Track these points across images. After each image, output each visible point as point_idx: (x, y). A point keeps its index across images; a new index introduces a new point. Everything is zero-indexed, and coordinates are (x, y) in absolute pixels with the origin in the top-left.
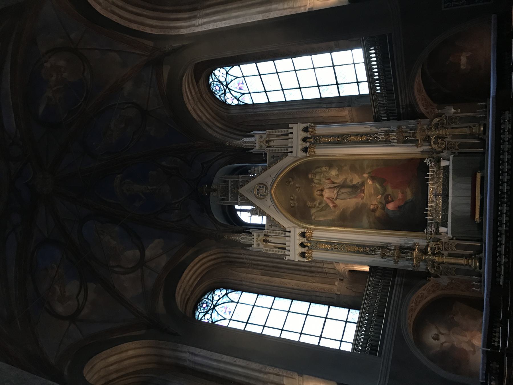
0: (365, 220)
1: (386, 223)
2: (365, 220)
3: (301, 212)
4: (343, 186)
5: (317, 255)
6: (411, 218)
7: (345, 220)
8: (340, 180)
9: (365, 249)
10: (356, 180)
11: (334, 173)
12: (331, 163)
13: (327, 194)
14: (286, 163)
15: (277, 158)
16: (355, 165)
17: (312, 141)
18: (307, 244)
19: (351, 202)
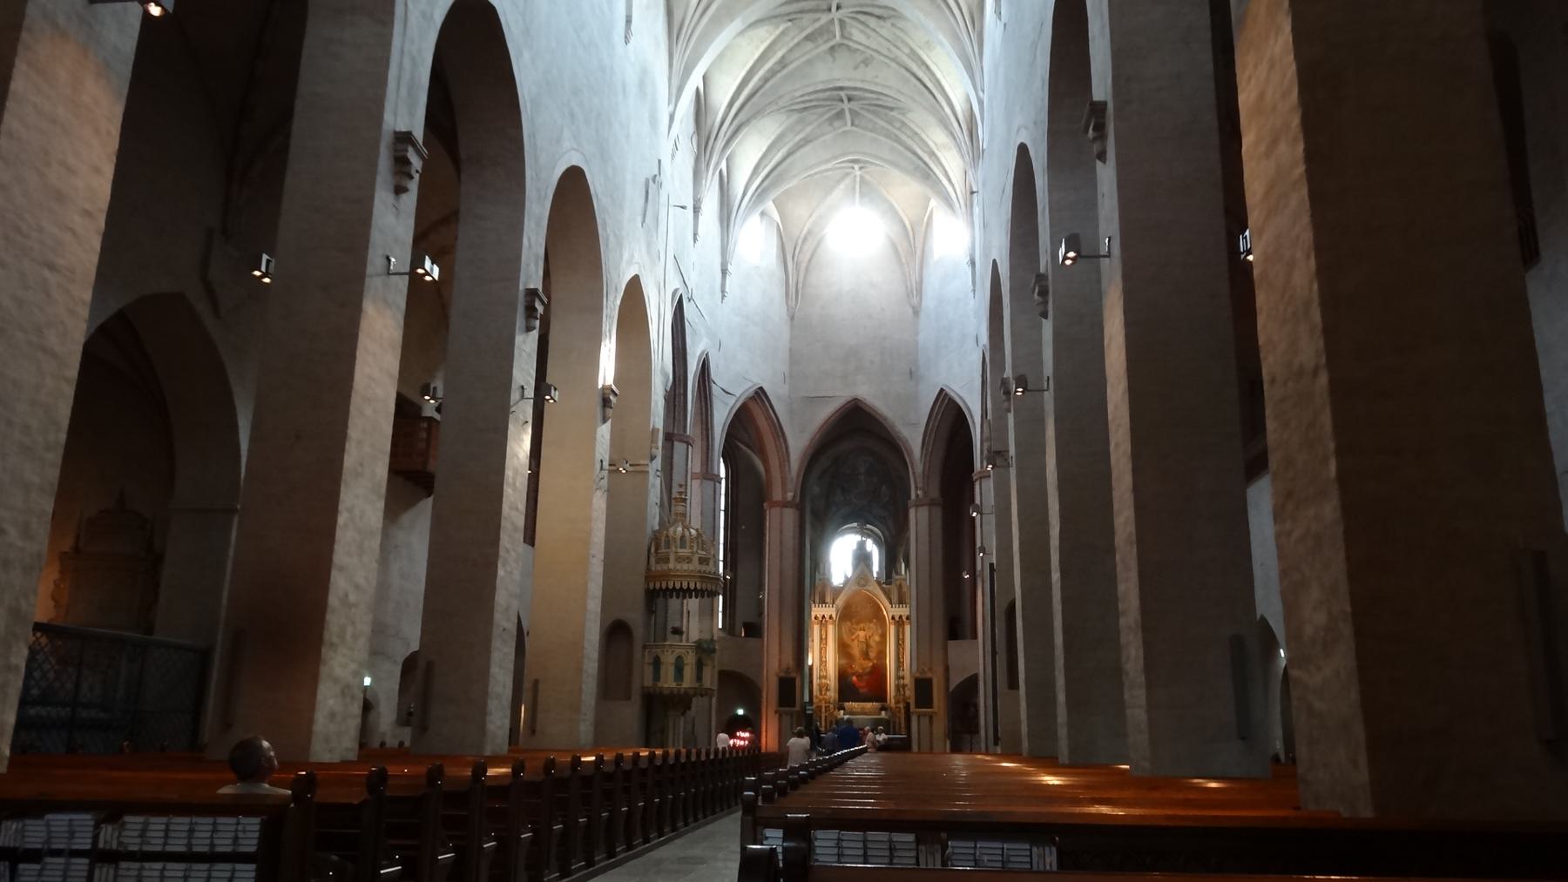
0: (844, 662)
1: (843, 676)
2: (844, 662)
3: (847, 615)
4: (868, 646)
5: (816, 628)
6: (847, 690)
7: (843, 648)
8: (872, 643)
9: (823, 662)
10: (872, 655)
11: (877, 638)
12: (883, 636)
13: (862, 634)
14: (883, 601)
15: (888, 594)
16: (882, 654)
17: (899, 623)
18: (823, 621)
19: (856, 651)
